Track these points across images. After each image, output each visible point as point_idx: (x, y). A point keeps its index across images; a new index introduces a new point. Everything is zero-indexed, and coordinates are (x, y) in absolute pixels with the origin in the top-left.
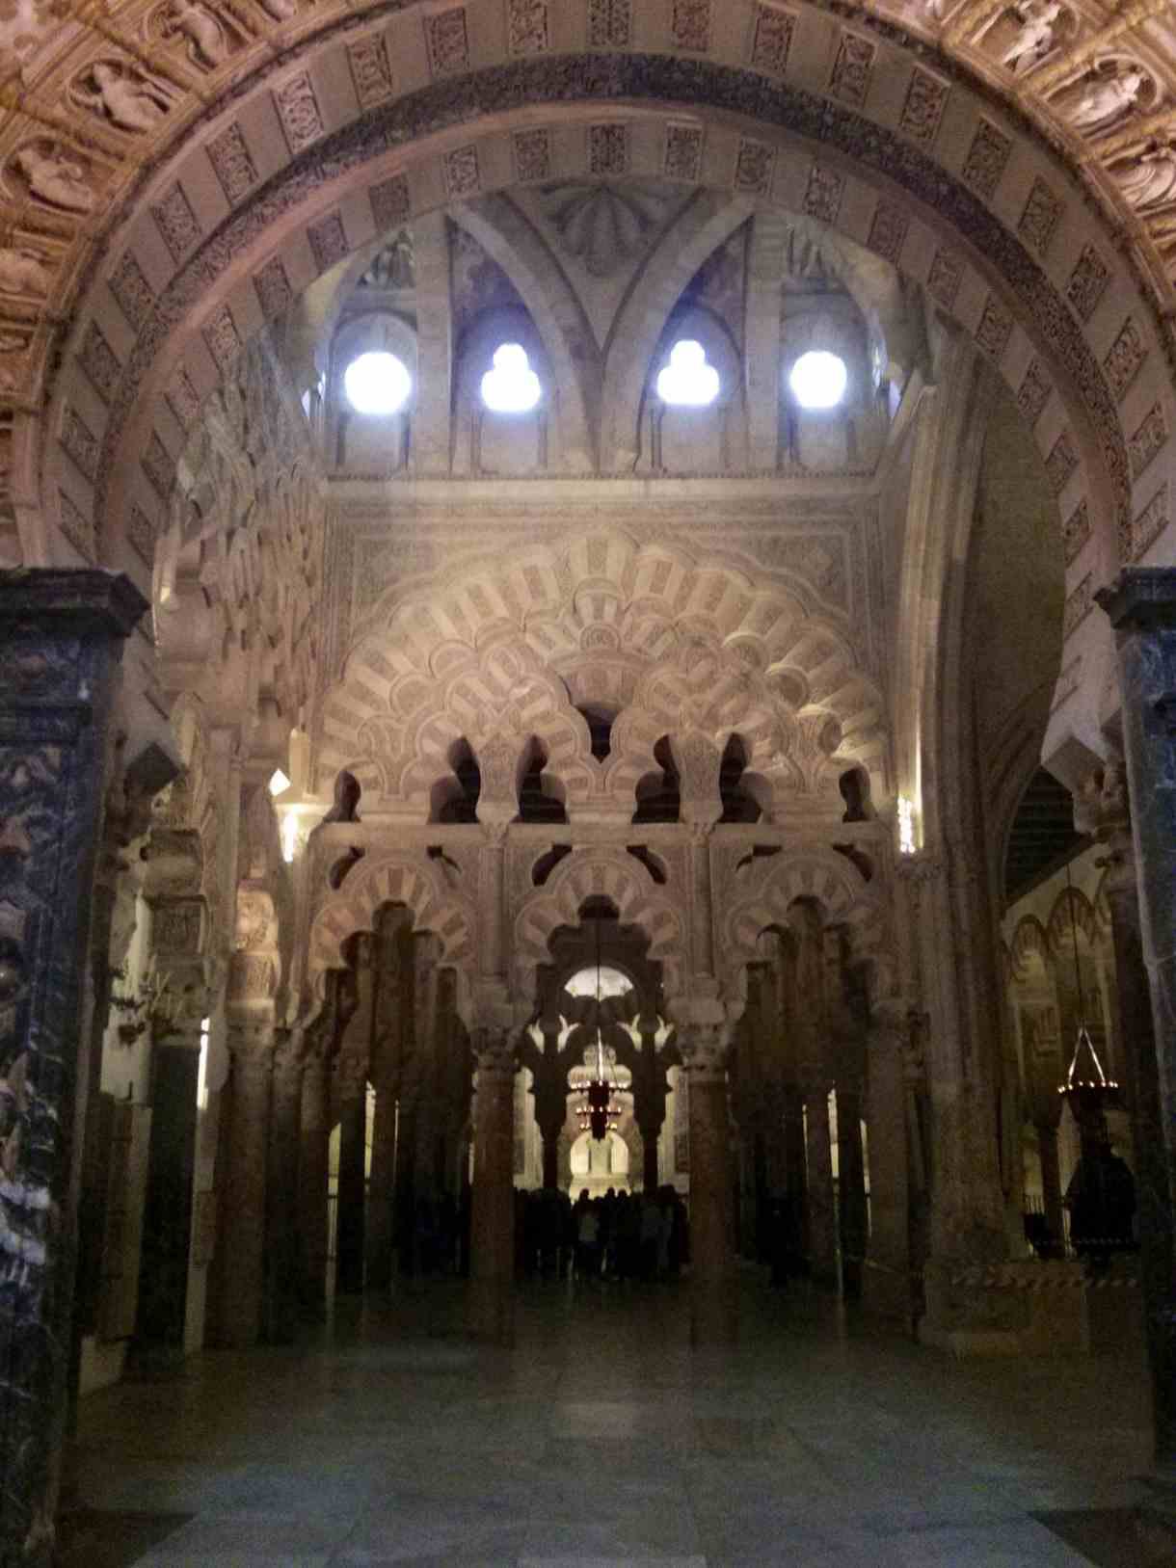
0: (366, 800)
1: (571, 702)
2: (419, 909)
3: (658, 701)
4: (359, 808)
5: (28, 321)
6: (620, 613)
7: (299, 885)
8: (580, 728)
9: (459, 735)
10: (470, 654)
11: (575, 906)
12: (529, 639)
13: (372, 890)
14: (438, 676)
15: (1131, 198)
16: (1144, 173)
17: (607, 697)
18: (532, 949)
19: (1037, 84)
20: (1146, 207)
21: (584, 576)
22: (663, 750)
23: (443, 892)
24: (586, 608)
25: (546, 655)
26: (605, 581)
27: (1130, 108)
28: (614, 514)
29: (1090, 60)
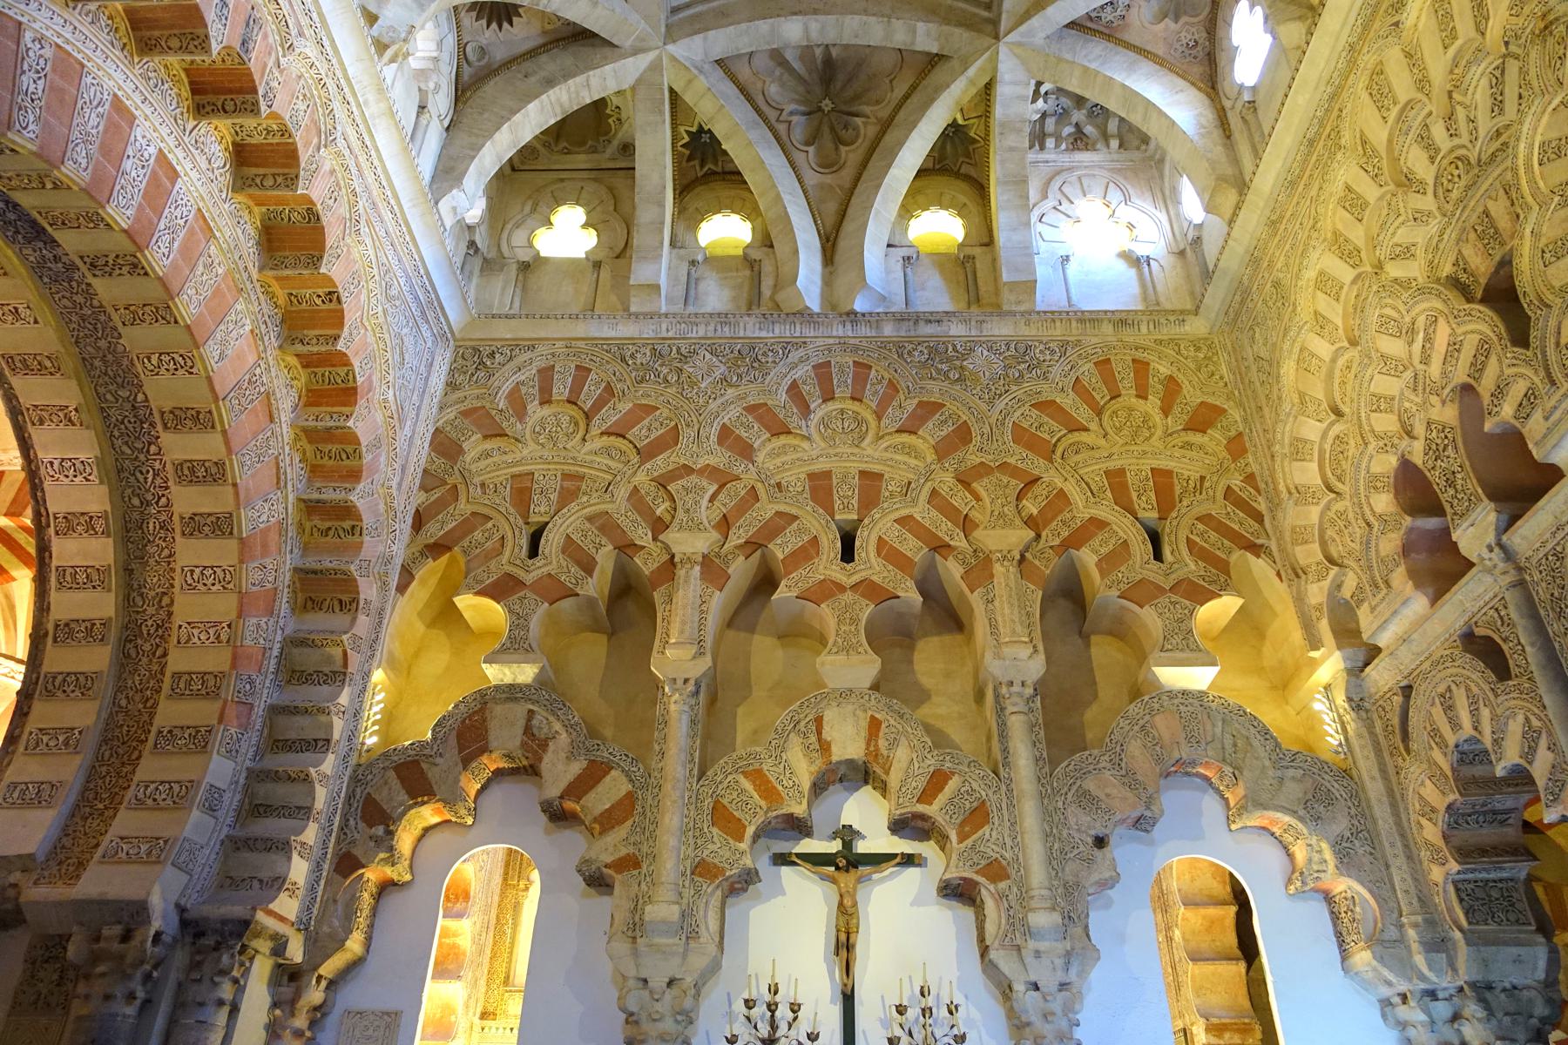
0: (1366, 620)
2: (1487, 741)
4: (1365, 636)
7: (1366, 766)
9: (1393, 461)
10: (1353, 353)
12: (1394, 270)
13: (1435, 733)
14: (1345, 409)
21: (1384, 136)
23: (1496, 696)
24: (1418, 163)
25: (1414, 270)
26: (1409, 104)
28: (1366, 27)
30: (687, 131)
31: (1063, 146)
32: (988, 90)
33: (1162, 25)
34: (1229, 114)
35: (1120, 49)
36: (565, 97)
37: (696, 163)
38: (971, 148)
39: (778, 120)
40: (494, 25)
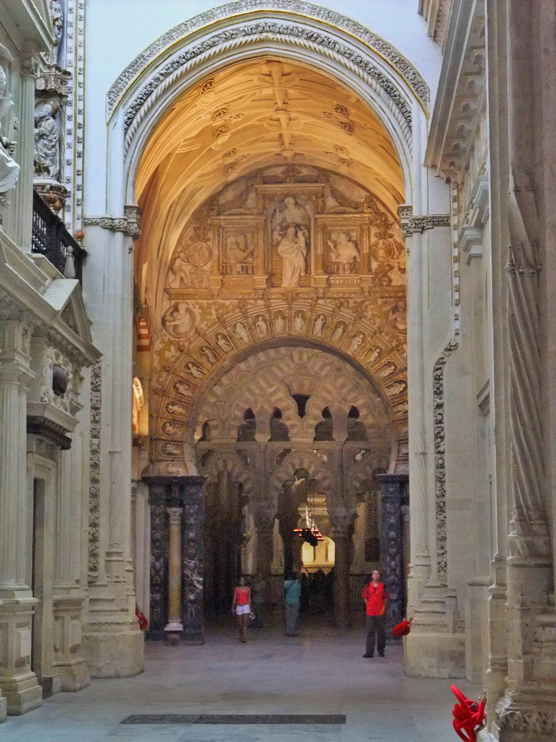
0: (214, 433)
1: (290, 393)
3: (325, 394)
5: (182, 422)
6: (309, 358)
8: (293, 404)
9: (248, 407)
11: (292, 473)
12: (275, 369)
13: (217, 465)
15: (388, 394)
16: (392, 389)
17: (305, 392)
18: (276, 489)
19: (374, 368)
20: (394, 395)
22: (326, 413)
27: (392, 373)
29: (385, 362)
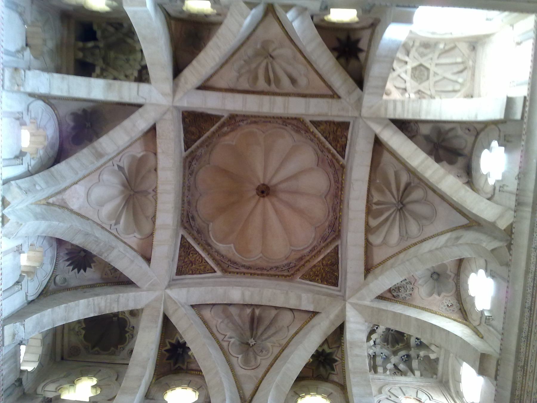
30: (170, 343)
31: (388, 372)
32: (340, 330)
33: (431, 298)
34: (479, 328)
35: (412, 308)
36: (103, 304)
37: (172, 362)
38: (334, 365)
39: (223, 340)
40: (76, 270)
